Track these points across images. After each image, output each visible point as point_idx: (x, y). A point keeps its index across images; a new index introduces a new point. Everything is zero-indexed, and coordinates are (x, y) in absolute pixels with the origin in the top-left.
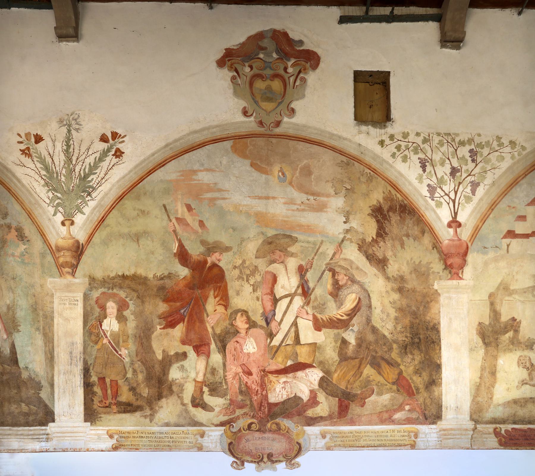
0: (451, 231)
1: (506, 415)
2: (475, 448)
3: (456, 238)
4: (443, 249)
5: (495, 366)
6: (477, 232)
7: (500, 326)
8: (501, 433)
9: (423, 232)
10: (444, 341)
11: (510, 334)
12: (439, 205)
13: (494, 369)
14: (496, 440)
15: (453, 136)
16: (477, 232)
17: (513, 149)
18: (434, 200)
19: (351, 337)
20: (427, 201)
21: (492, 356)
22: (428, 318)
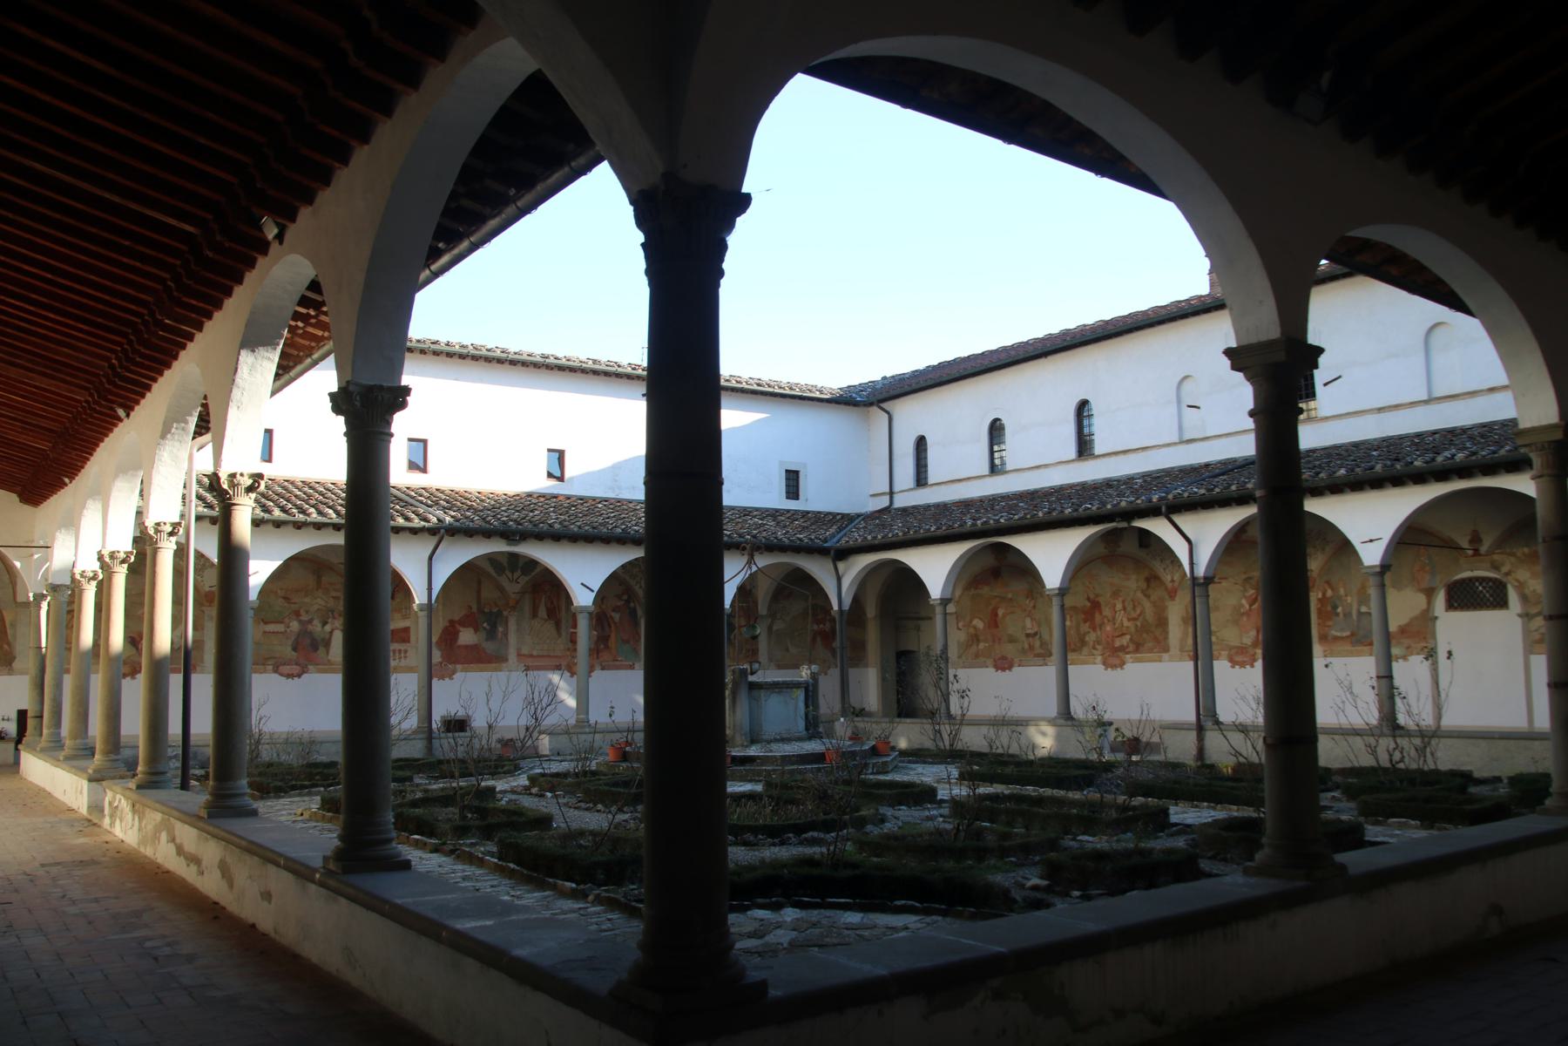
19: (1139, 624)
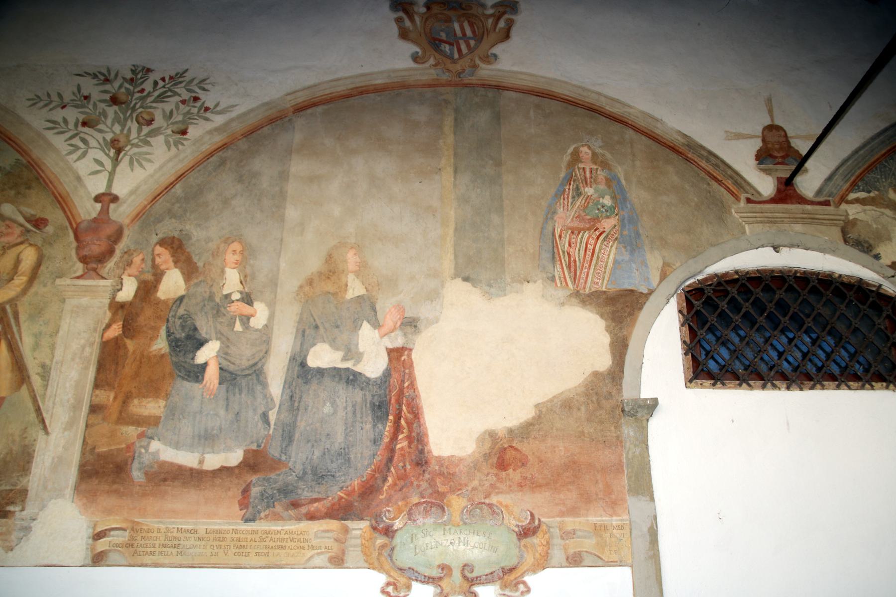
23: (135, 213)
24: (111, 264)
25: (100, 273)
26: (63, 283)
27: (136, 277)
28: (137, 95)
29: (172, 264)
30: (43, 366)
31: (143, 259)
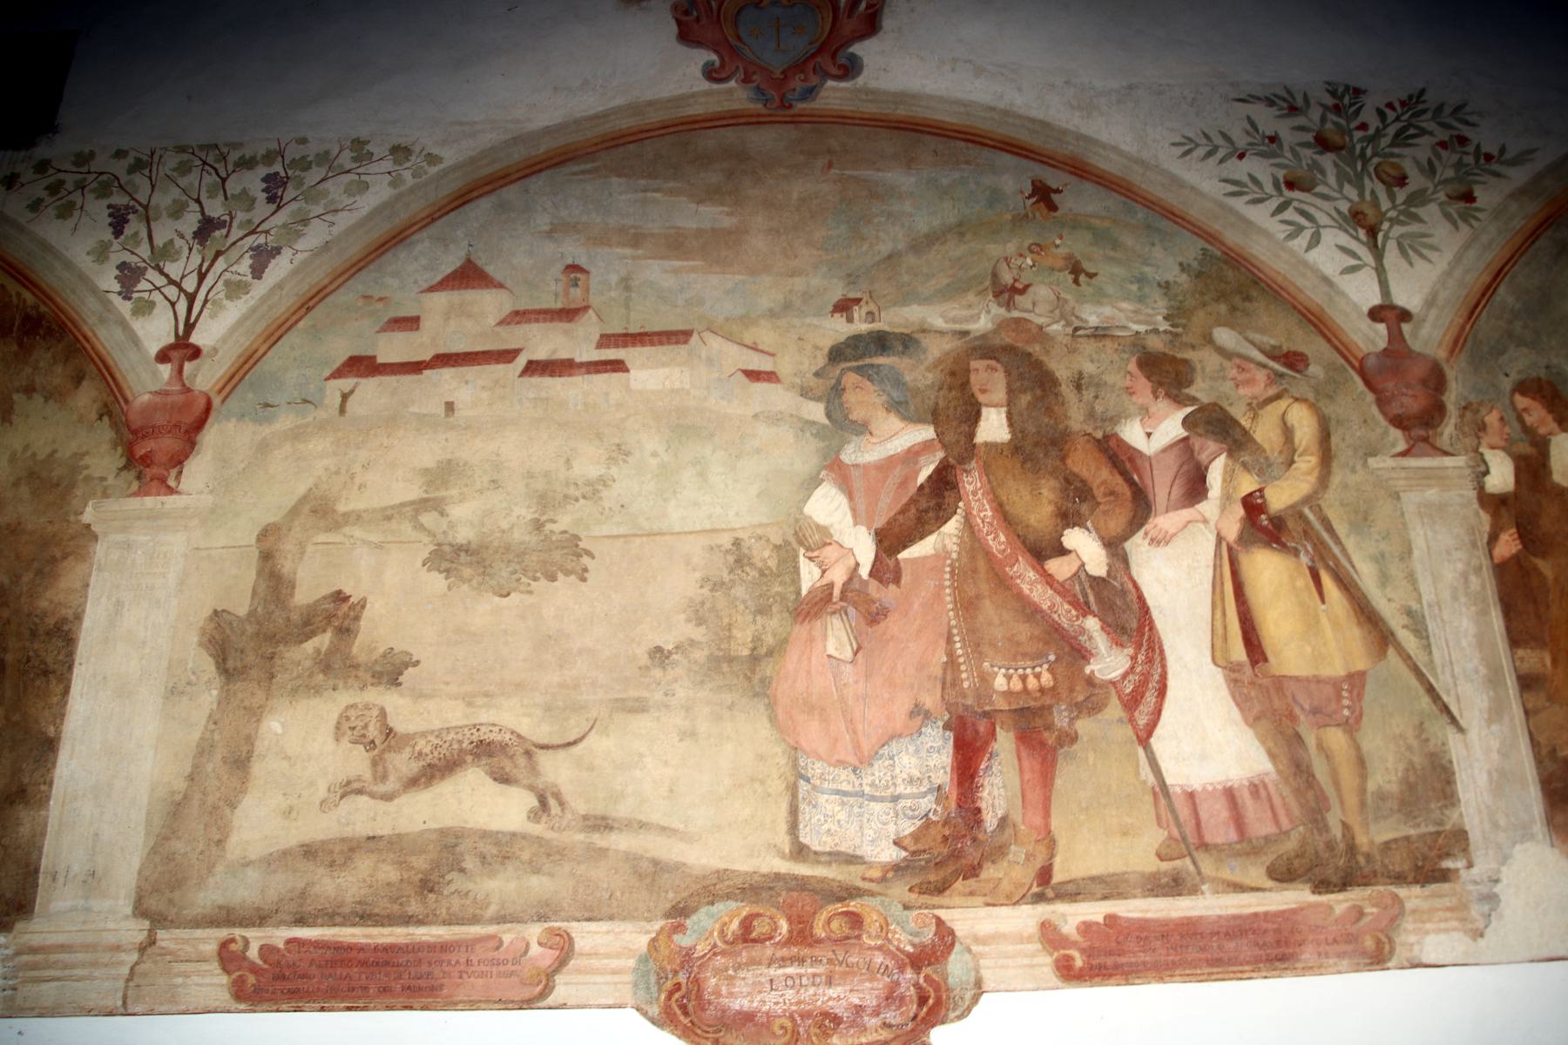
0: (166, 370)
1: (272, 895)
2: (137, 1010)
3: (177, 388)
4: (132, 417)
5: (250, 740)
6: (247, 366)
7: (288, 619)
8: (245, 958)
9: (78, 379)
10: (83, 668)
11: (324, 640)
12: (145, 308)
13: (245, 749)
14: (224, 979)
15: (225, 150)
16: (247, 366)
17: (401, 164)
18: (130, 299)
20: (110, 302)
21: (245, 708)
22: (43, 604)
23: (1449, 338)
24: (1448, 431)
25: (1438, 444)
26: (1382, 465)
27: (1503, 449)
28: (1358, 135)
29: (1554, 426)
30: (1409, 613)
31: (1502, 419)
